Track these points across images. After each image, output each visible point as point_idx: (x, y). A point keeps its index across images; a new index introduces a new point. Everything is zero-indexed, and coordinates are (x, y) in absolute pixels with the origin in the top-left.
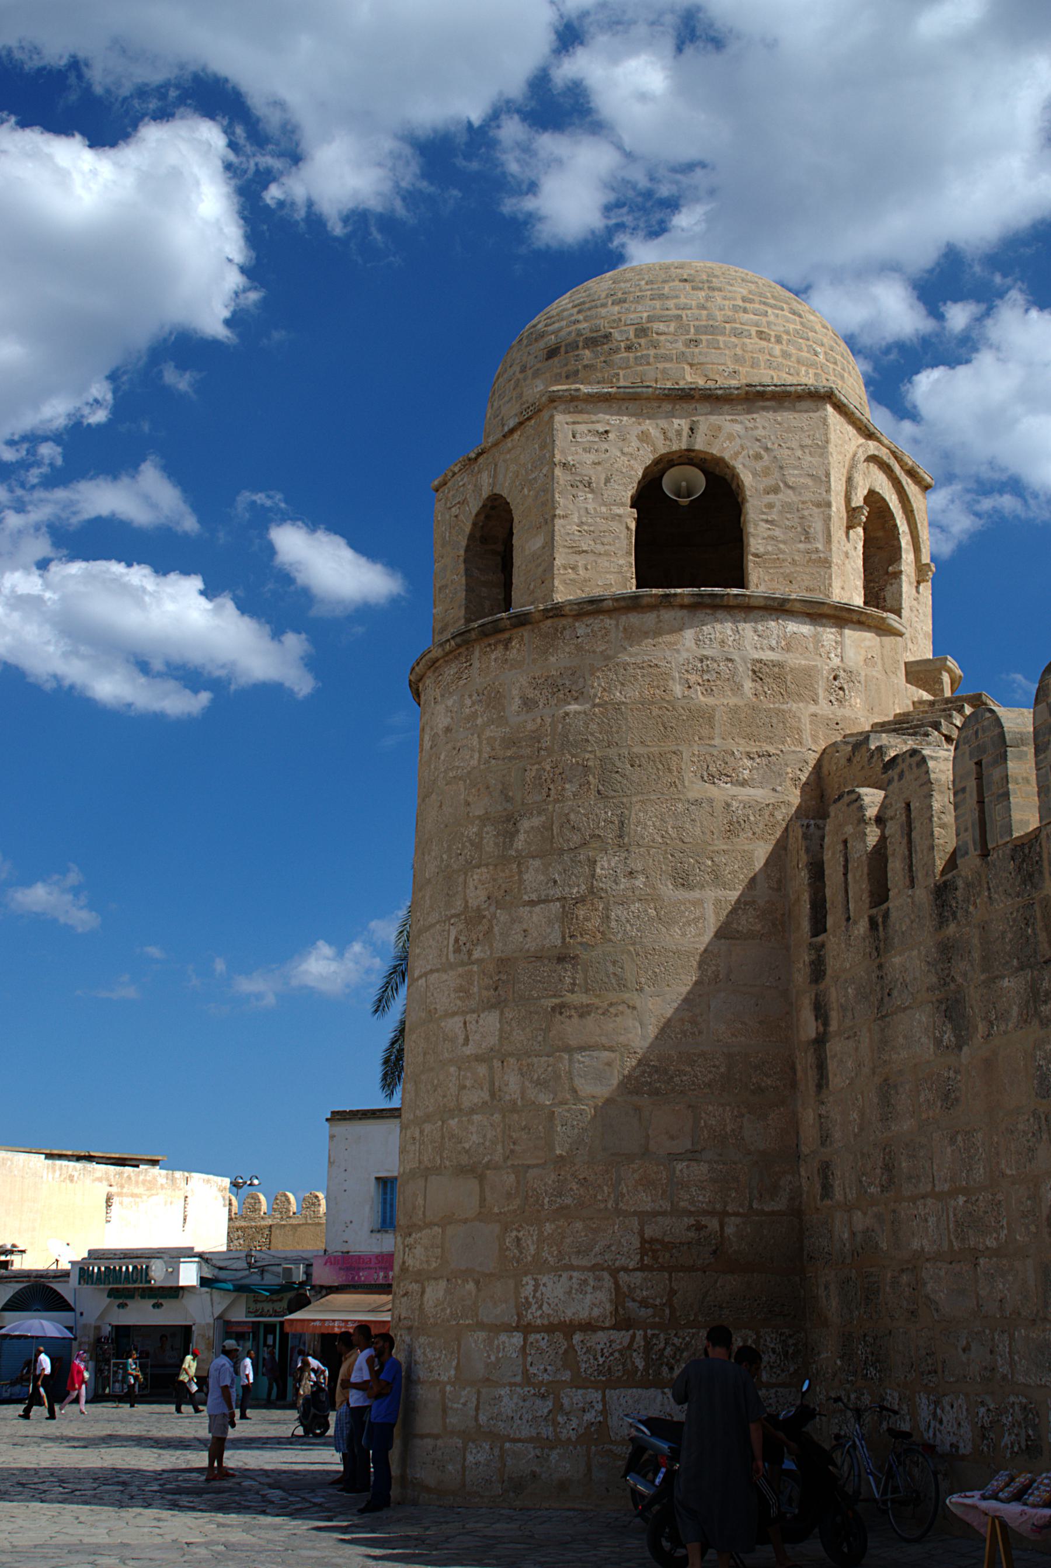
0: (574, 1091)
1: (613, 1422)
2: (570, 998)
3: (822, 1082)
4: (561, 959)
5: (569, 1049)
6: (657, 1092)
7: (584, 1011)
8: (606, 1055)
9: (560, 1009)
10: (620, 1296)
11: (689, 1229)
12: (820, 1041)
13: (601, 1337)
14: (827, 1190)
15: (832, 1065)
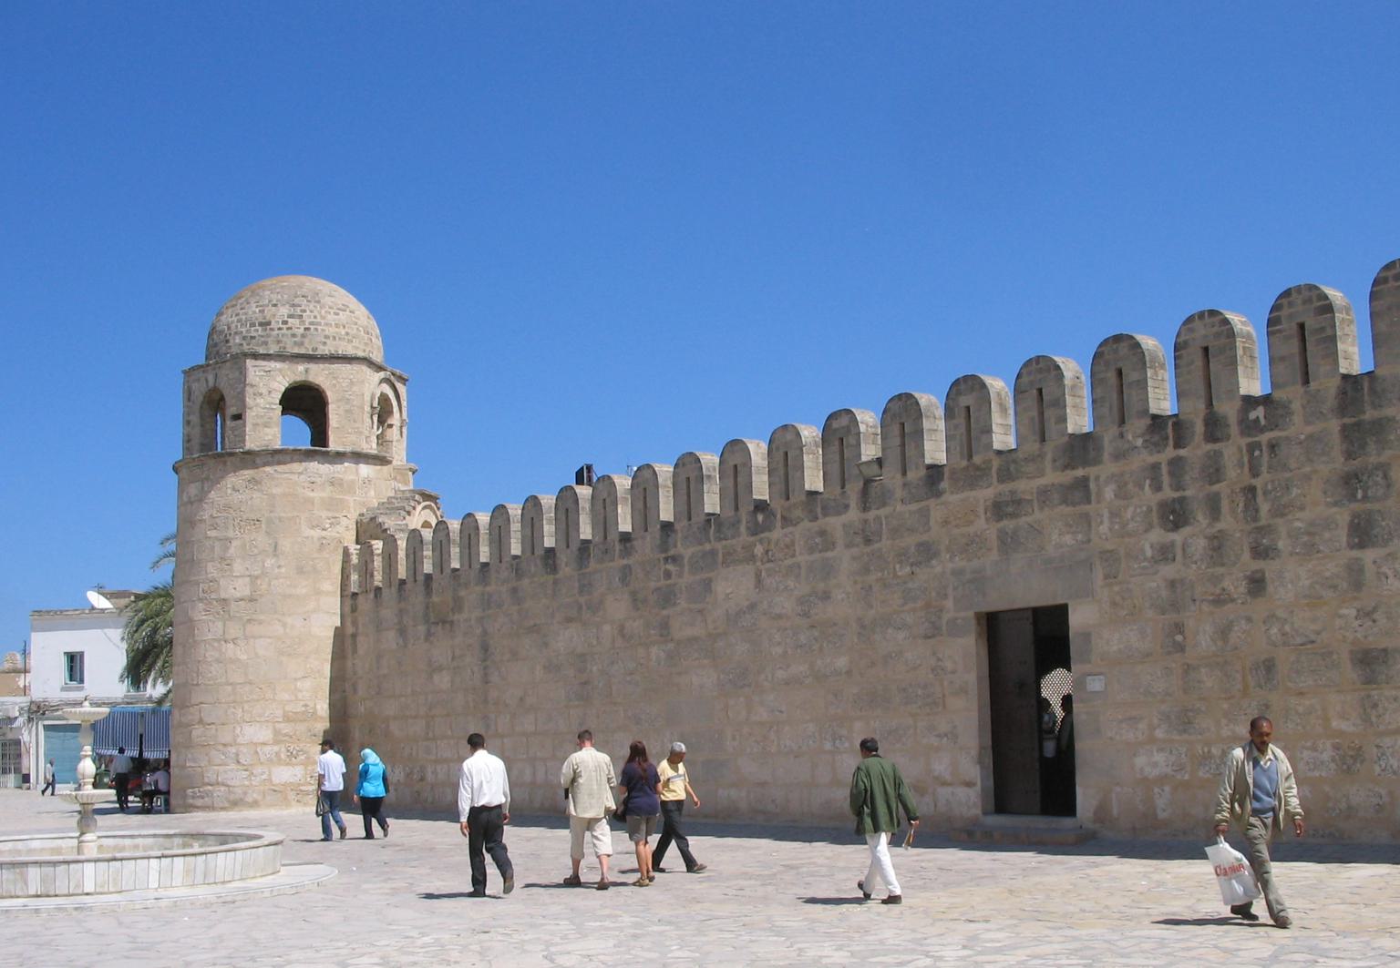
0: (256, 654)
1: (274, 779)
2: (254, 616)
3: (355, 651)
4: (251, 601)
5: (254, 637)
6: (289, 655)
7: (261, 623)
8: (269, 640)
9: (249, 621)
10: (276, 732)
11: (303, 706)
12: (354, 636)
13: (267, 749)
14: (355, 691)
15: (359, 646)
